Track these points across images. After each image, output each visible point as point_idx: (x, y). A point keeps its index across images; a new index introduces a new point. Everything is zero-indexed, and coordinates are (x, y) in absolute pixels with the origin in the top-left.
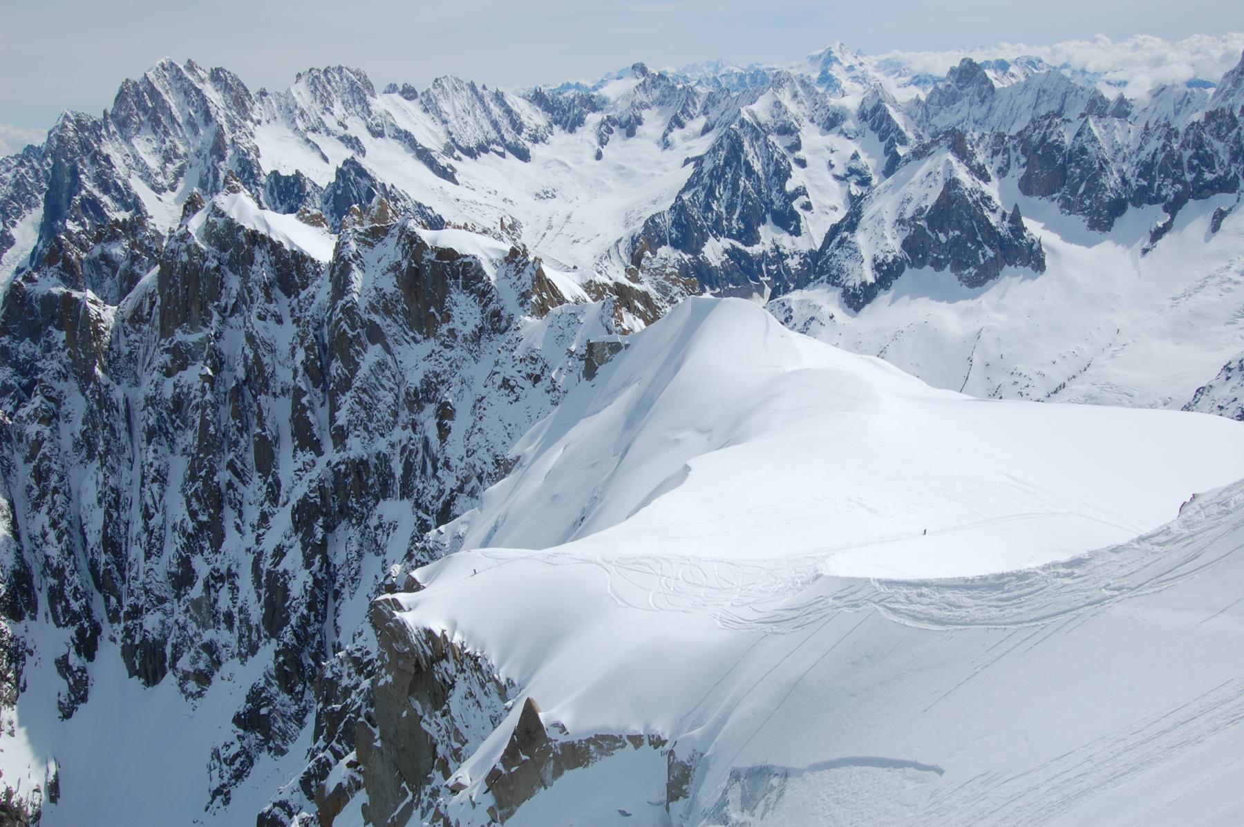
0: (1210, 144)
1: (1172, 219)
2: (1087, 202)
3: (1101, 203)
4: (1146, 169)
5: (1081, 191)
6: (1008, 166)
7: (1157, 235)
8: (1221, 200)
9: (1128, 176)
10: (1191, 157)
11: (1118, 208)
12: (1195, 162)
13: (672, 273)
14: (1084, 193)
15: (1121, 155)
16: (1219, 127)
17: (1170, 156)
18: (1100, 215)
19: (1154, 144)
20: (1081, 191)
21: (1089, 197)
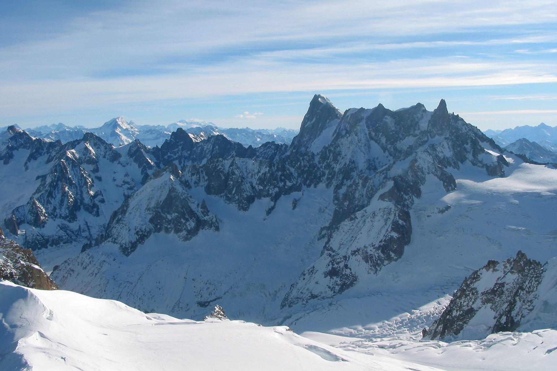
0: (289, 170)
1: (275, 205)
2: (237, 197)
3: (244, 198)
4: (262, 181)
5: (234, 192)
6: (199, 180)
7: (270, 211)
8: (295, 195)
9: (254, 185)
10: (281, 176)
11: (251, 200)
12: (283, 178)
13: (17, 246)
14: (235, 193)
15: (250, 175)
16: (292, 162)
17: (272, 175)
18: (243, 203)
19: (265, 169)
20: (234, 192)
21: (238, 195)
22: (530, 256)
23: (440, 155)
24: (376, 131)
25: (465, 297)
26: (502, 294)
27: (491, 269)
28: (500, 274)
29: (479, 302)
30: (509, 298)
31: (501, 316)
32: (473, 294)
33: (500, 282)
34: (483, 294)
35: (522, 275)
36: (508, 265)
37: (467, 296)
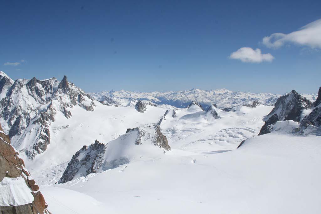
22: (101, 142)
23: (64, 102)
24: (32, 90)
25: (74, 164)
26: (89, 160)
27: (85, 150)
28: (88, 151)
29: (79, 166)
30: (92, 162)
31: (89, 170)
32: (77, 162)
33: (88, 155)
34: (81, 161)
35: (98, 150)
36: (92, 147)
37: (74, 163)
